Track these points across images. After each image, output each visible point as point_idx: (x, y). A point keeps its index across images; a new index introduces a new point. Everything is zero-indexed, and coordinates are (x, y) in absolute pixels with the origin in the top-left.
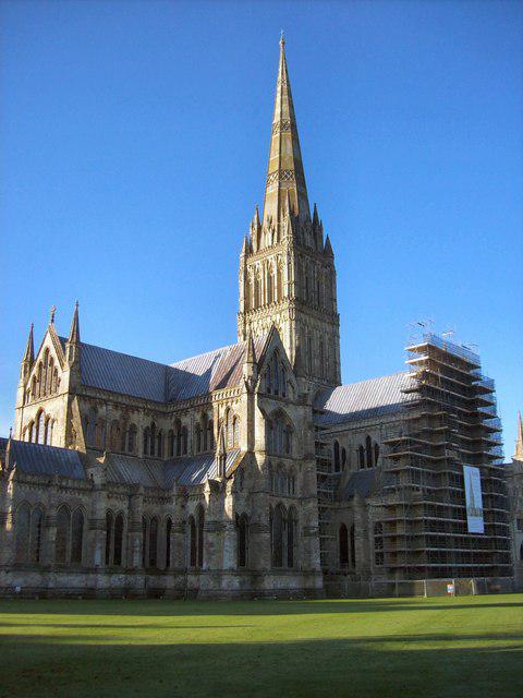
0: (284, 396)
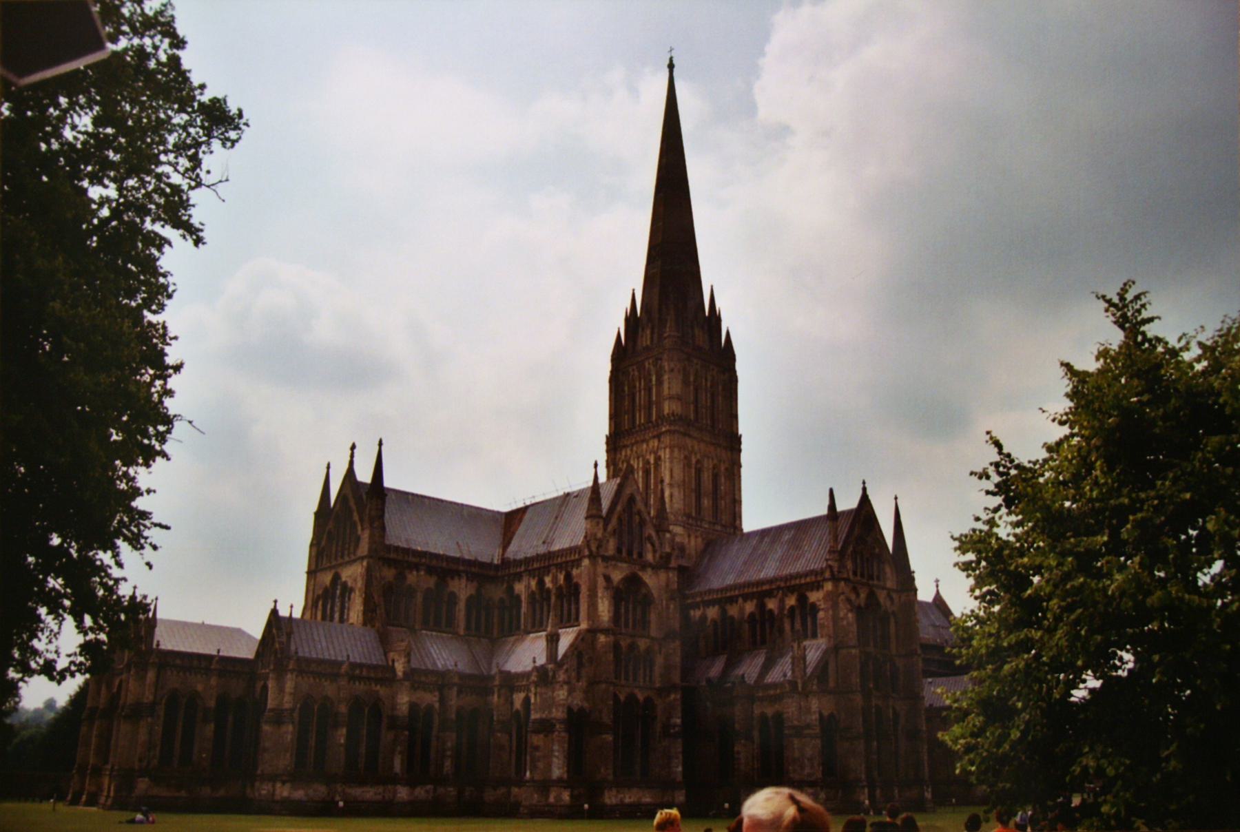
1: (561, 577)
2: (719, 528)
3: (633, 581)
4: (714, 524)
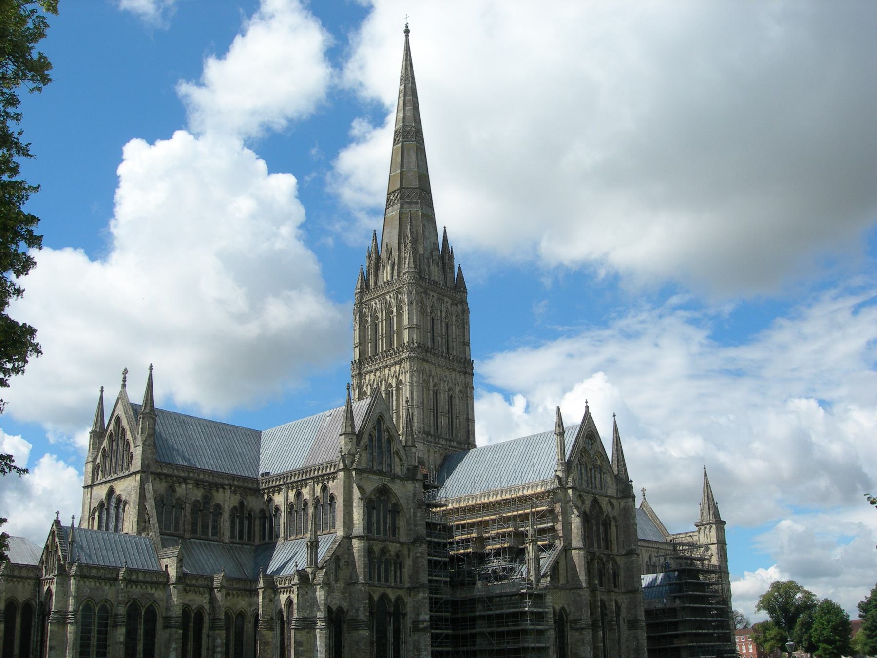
1: (318, 488)
2: (455, 444)
4: (450, 441)
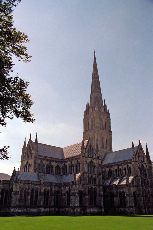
0: (93, 157)
3: (91, 162)
